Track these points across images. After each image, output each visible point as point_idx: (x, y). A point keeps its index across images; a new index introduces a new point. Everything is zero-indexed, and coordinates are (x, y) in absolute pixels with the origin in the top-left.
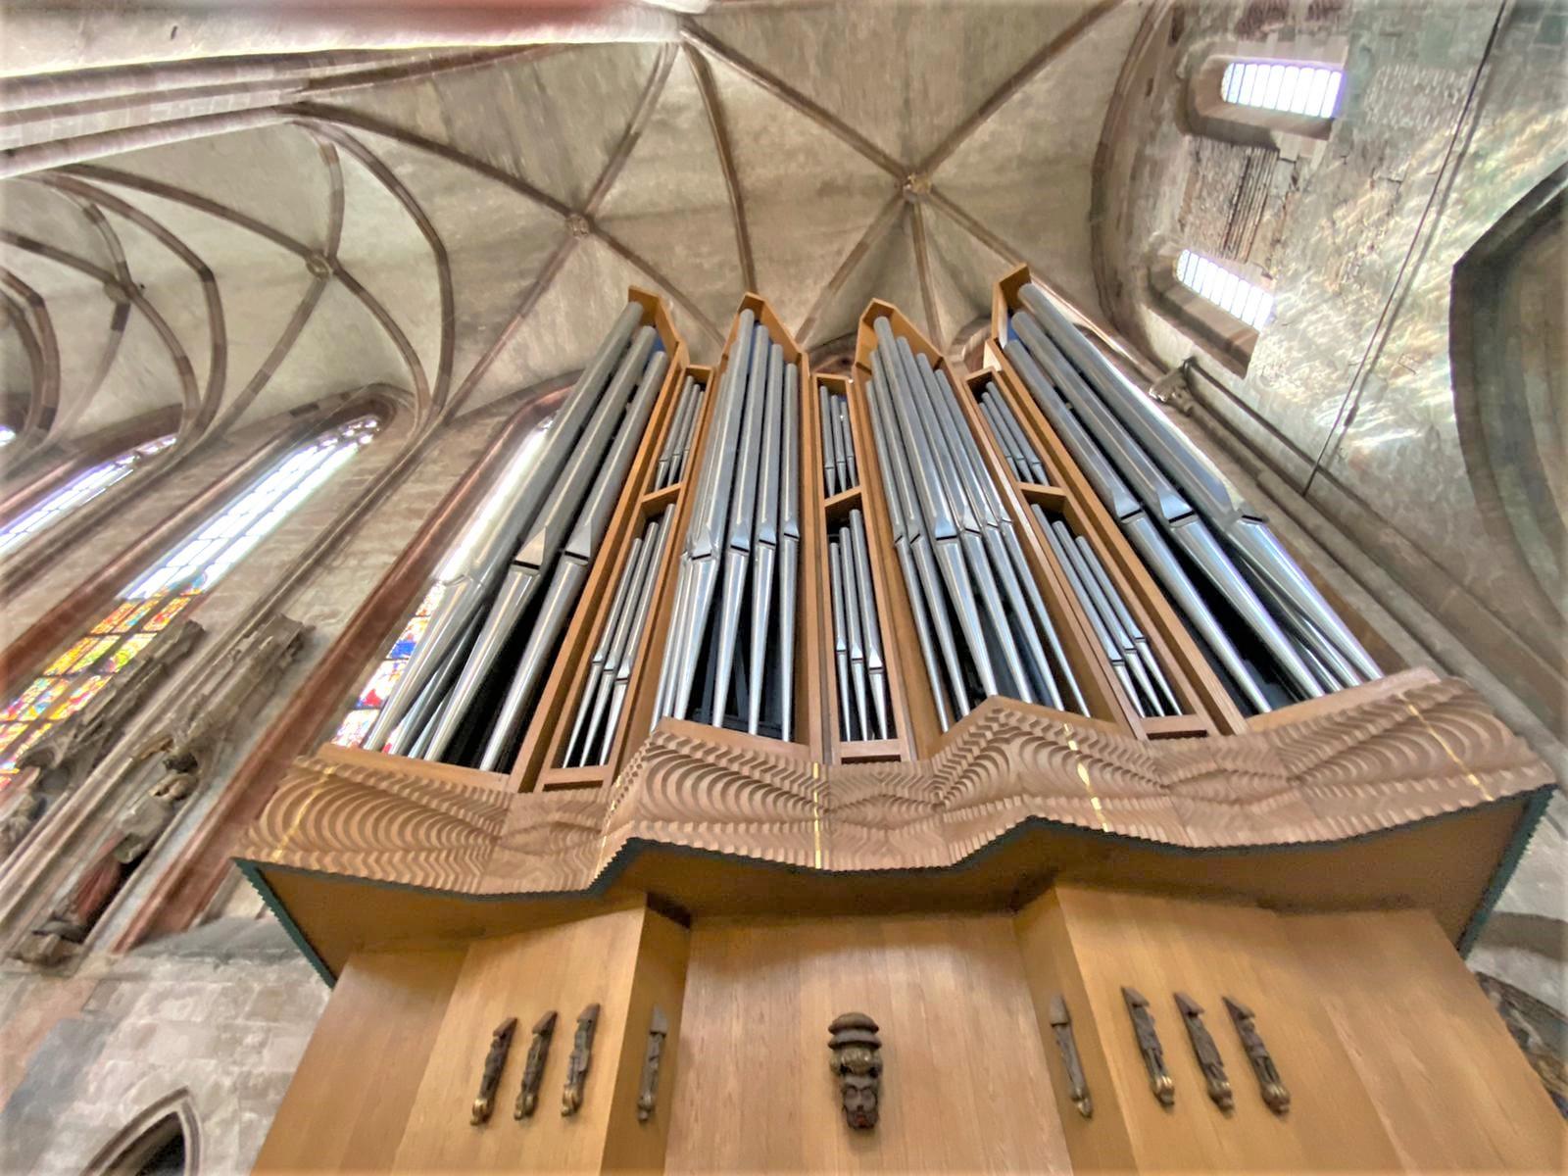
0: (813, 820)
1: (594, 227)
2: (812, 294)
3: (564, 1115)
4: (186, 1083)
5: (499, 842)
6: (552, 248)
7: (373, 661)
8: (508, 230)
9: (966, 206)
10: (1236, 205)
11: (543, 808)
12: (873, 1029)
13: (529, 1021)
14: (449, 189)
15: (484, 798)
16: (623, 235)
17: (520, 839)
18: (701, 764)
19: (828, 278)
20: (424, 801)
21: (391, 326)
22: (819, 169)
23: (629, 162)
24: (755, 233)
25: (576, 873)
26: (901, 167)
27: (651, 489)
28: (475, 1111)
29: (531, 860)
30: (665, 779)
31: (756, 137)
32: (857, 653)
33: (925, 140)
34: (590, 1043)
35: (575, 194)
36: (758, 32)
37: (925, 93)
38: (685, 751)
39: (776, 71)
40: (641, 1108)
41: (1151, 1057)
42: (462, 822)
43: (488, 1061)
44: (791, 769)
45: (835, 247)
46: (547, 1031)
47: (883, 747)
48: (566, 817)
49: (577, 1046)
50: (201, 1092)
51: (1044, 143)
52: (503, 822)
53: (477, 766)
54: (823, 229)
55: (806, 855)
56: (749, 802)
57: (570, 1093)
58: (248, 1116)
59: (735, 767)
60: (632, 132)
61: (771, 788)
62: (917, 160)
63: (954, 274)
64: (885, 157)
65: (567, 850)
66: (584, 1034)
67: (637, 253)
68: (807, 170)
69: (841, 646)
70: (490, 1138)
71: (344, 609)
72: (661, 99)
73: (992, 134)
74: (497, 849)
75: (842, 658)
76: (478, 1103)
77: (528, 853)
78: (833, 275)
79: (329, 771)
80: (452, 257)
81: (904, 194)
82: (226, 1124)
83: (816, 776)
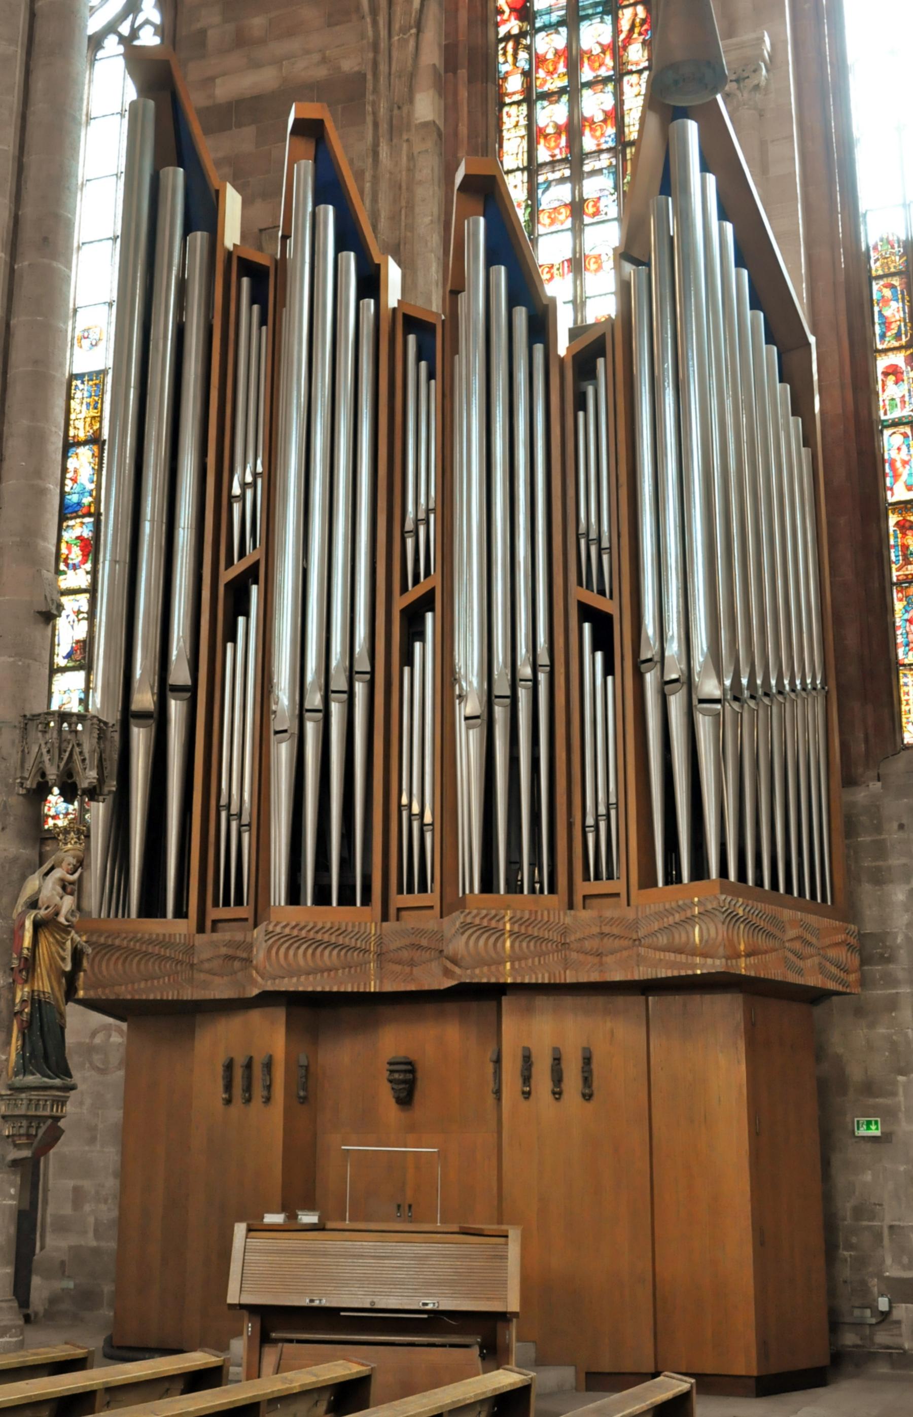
0: (370, 962)
3: (264, 1102)
5: (195, 967)
12: (410, 1063)
15: (178, 940)
17: (207, 966)
18: (297, 939)
20: (144, 949)
27: (230, 563)
28: (223, 1099)
29: (217, 980)
30: (277, 953)
32: (416, 809)
38: (287, 931)
41: (527, 1079)
42: (169, 958)
43: (224, 1078)
44: (356, 930)
46: (249, 1066)
48: (230, 952)
49: (264, 1075)
52: (193, 954)
55: (365, 984)
56: (329, 957)
59: (319, 937)
61: (343, 947)
65: (236, 973)
66: (265, 1069)
69: (405, 800)
74: (195, 971)
75: (405, 814)
76: (224, 1096)
83: (373, 932)
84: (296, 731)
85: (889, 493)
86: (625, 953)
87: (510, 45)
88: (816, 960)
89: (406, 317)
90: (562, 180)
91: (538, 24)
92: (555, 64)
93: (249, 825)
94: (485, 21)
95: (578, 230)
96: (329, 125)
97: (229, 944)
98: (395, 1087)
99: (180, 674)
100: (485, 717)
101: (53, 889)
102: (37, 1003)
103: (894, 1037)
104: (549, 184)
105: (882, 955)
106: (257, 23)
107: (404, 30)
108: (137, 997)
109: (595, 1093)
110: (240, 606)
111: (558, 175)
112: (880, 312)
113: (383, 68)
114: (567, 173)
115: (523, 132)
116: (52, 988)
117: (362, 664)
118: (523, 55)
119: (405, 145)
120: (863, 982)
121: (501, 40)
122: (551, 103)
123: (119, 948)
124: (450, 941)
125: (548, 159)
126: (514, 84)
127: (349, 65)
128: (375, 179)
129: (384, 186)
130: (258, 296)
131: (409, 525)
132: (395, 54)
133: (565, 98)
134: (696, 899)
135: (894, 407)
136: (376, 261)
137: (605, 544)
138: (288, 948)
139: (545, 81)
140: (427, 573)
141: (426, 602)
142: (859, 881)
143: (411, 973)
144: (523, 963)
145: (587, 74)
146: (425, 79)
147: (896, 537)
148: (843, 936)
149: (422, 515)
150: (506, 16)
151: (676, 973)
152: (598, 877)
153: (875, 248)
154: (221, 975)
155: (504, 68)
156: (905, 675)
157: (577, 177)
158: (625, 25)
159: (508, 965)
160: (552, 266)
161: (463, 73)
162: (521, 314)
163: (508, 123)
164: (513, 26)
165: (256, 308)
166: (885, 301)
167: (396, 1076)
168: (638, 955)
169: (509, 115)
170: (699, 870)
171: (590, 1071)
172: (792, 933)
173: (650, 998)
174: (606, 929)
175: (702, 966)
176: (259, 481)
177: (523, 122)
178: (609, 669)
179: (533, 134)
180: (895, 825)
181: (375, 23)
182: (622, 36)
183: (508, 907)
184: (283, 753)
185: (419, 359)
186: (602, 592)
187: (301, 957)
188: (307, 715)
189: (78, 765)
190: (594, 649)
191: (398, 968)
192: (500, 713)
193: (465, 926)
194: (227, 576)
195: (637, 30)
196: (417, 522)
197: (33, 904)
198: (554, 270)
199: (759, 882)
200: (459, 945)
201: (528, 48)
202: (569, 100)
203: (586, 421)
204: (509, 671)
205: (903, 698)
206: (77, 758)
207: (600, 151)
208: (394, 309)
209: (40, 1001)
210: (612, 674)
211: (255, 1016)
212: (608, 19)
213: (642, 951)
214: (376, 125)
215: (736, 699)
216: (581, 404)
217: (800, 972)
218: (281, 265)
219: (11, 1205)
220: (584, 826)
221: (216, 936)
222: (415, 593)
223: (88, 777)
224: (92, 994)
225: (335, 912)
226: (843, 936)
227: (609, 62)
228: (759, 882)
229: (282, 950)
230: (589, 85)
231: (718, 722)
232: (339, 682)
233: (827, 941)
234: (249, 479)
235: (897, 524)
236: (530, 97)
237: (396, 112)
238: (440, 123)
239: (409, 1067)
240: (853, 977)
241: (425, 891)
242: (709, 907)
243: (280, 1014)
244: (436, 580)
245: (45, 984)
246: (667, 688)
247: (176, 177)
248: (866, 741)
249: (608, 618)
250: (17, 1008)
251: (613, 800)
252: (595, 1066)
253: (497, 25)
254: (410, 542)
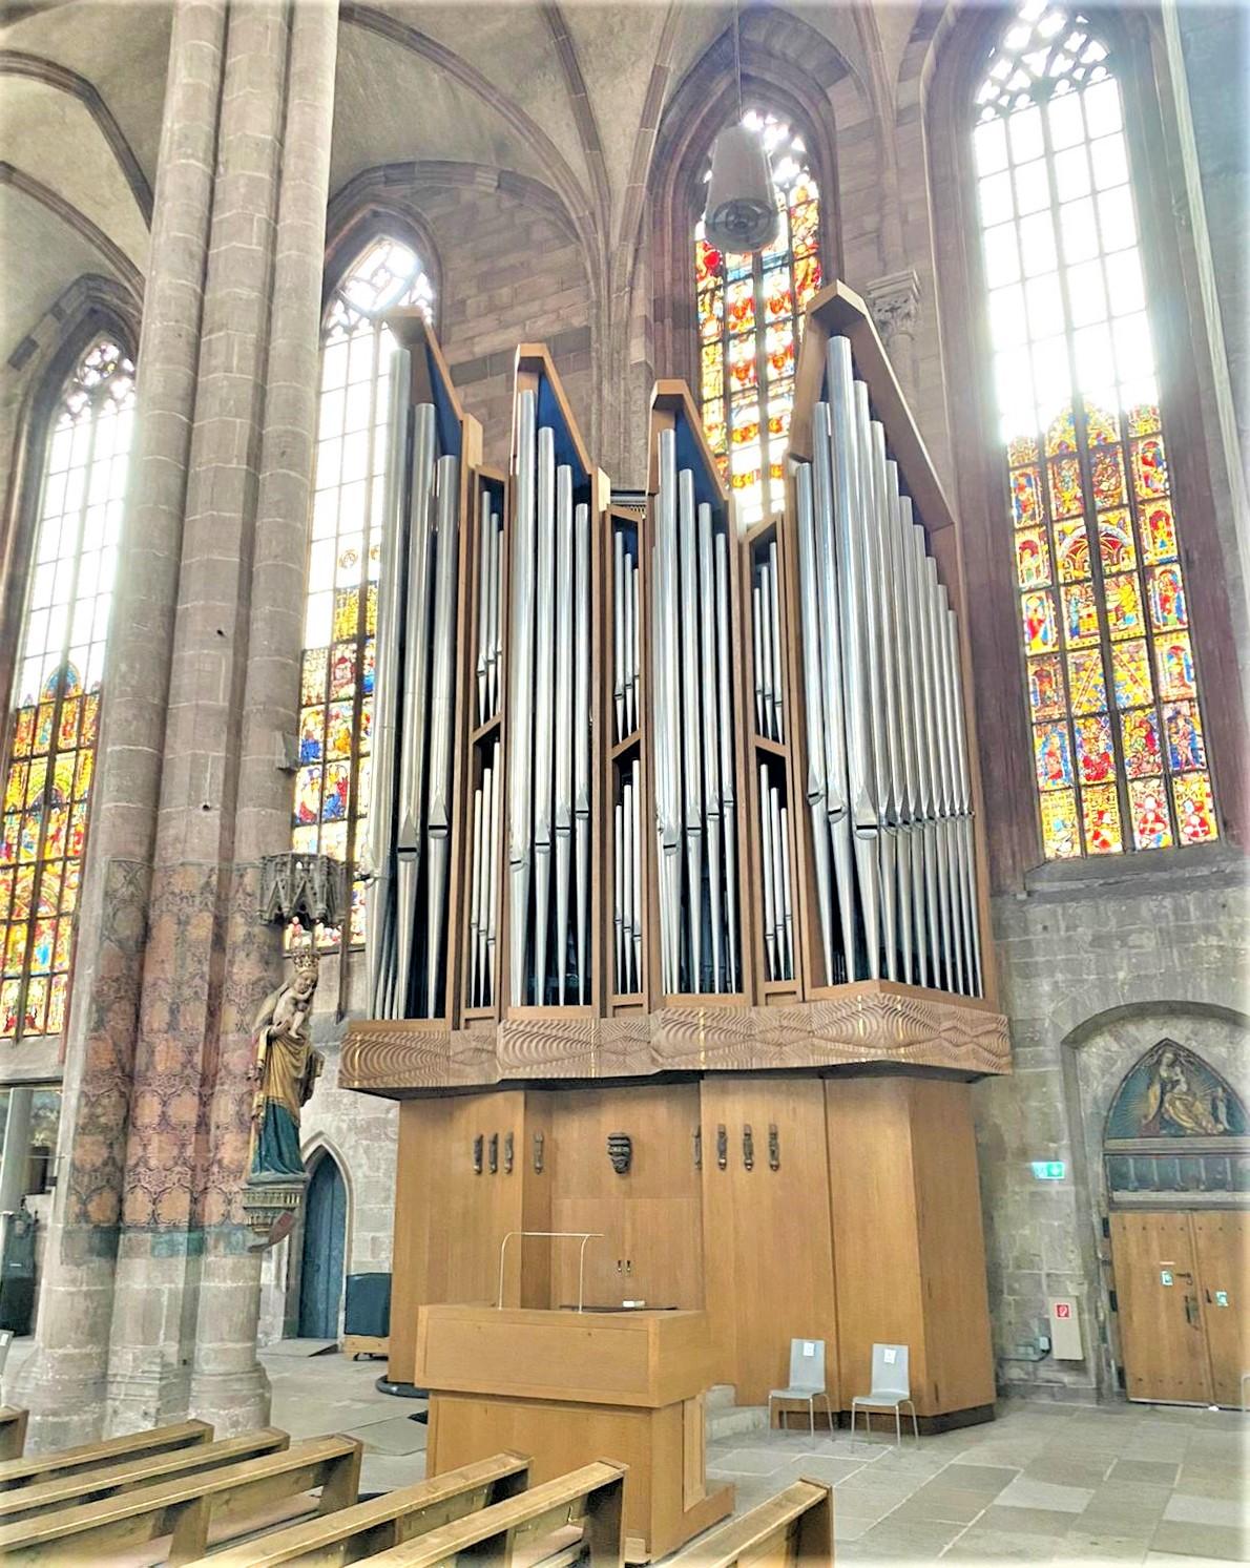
4: (322, 1129)
12: (628, 1139)
17: (460, 1057)
21: (76, 220)
27: (477, 725)
38: (521, 1028)
41: (723, 1153)
46: (495, 1142)
50: (331, 1132)
53: (427, 1017)
56: (556, 1049)
58: (365, 1142)
65: (482, 1063)
79: (359, 1038)
82: (355, 1147)
84: (528, 862)
85: (1027, 648)
87: (708, 295)
88: (971, 1046)
89: (614, 518)
90: (751, 404)
91: (730, 279)
92: (744, 309)
93: (494, 939)
94: (686, 281)
95: (765, 442)
96: (548, 362)
97: (477, 1039)
98: (616, 1159)
99: (437, 816)
100: (680, 846)
101: (285, 1008)
102: (271, 1107)
103: (1046, 1110)
104: (740, 408)
105: (1032, 1039)
106: (505, 293)
107: (619, 289)
108: (403, 1085)
109: (782, 1163)
110: (488, 762)
111: (747, 401)
112: (1017, 497)
113: (604, 320)
114: (755, 398)
115: (720, 367)
116: (284, 1093)
117: (582, 805)
118: (718, 305)
119: (622, 382)
120: (1014, 1064)
121: (700, 294)
122: (741, 342)
123: (388, 1044)
124: (655, 1034)
125: (739, 388)
126: (710, 330)
127: (578, 322)
128: (600, 411)
129: (606, 416)
130: (497, 507)
131: (619, 690)
132: (613, 309)
133: (753, 337)
134: (859, 998)
135: (1030, 576)
136: (589, 472)
137: (778, 698)
138: (523, 1042)
139: (734, 327)
140: (634, 728)
141: (633, 752)
142: (1010, 975)
144: (715, 1052)
145: (769, 317)
146: (637, 328)
147: (1034, 684)
148: (995, 1025)
149: (629, 681)
150: (703, 274)
151: (845, 1062)
152: (778, 978)
153: (1012, 446)
154: (471, 1065)
155: (702, 316)
156: (1046, 800)
157: (763, 400)
158: (800, 275)
159: (703, 1054)
160: (743, 477)
161: (668, 321)
162: (705, 509)
163: (706, 360)
164: (709, 282)
165: (495, 516)
166: (1021, 488)
167: (615, 1149)
168: (813, 1045)
169: (707, 354)
170: (863, 973)
171: (776, 1145)
172: (947, 1024)
173: (827, 1082)
174: (785, 1023)
175: (866, 1056)
176: (500, 658)
177: (719, 359)
178: (782, 803)
179: (727, 370)
180: (1040, 927)
181: (597, 285)
182: (798, 284)
183: (702, 1005)
184: (518, 879)
185: (625, 552)
186: (775, 739)
187: (534, 1049)
188: (537, 848)
189: (310, 899)
190: (770, 787)
191: (614, 1057)
192: (693, 842)
193: (666, 1021)
194: (474, 737)
195: (809, 278)
196: (625, 686)
197: (270, 1022)
198: (746, 479)
199: (916, 981)
200: (660, 1037)
201: (722, 298)
202: (756, 339)
203: (761, 596)
204: (699, 808)
205: (1045, 819)
206: (308, 892)
207: (782, 379)
208: (604, 512)
209: (274, 1106)
210: (786, 806)
211: (499, 1097)
212: (786, 270)
213: (816, 1041)
214: (600, 368)
215: (891, 824)
216: (756, 582)
217: (956, 1059)
218: (513, 480)
219: (230, 1293)
220: (765, 935)
221: (467, 1032)
222: (624, 745)
223: (317, 909)
224: (365, 1085)
225: (562, 1011)
226: (995, 1025)
227: (788, 305)
228: (916, 981)
229: (518, 1044)
230: (772, 325)
231: (877, 844)
232: (563, 820)
233: (980, 1030)
234: (491, 657)
235: (1036, 673)
236: (725, 339)
237: (616, 355)
238: (651, 363)
239: (625, 1142)
240: (1004, 1060)
241: (636, 991)
242: (871, 1004)
243: (519, 1096)
244: (641, 734)
245: (277, 1090)
246: (831, 817)
247: (427, 411)
248: (1013, 856)
249: (782, 760)
250: (254, 1113)
251: (788, 912)
252: (780, 1140)
253: (696, 282)
254: (620, 704)
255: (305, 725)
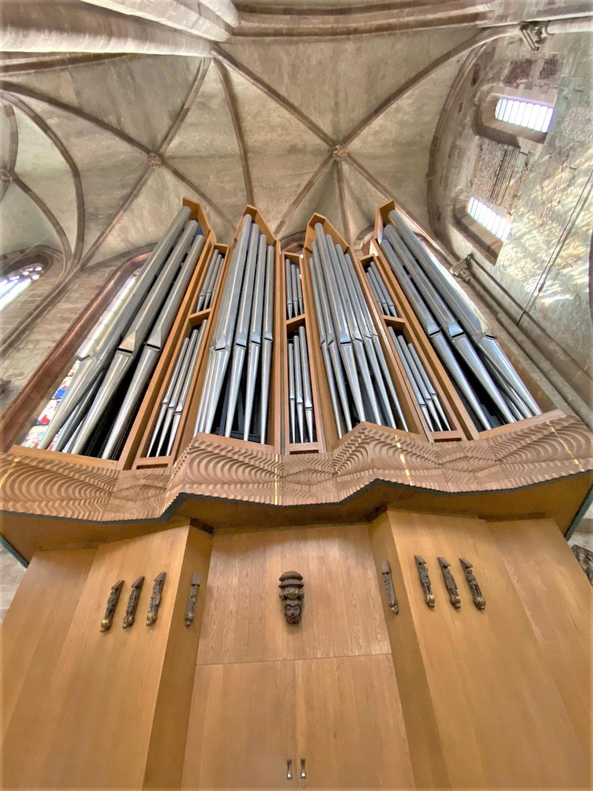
0: (275, 482)
1: (164, 162)
2: (284, 207)
3: (148, 625)
5: (113, 495)
6: (140, 172)
7: (45, 400)
8: (114, 160)
9: (366, 164)
10: (498, 175)
11: (136, 478)
12: (300, 578)
13: (130, 581)
14: (80, 134)
15: (104, 473)
16: (180, 167)
17: (124, 493)
18: (218, 456)
19: (292, 201)
22: (288, 138)
23: (183, 125)
24: (255, 173)
25: (154, 509)
26: (333, 141)
27: (194, 311)
28: (102, 626)
31: (255, 117)
32: (300, 400)
33: (345, 126)
34: (161, 590)
35: (153, 140)
36: (256, 55)
37: (346, 100)
38: (210, 449)
39: (266, 79)
40: (187, 620)
43: (109, 602)
44: (264, 457)
45: (296, 183)
46: (139, 586)
47: (311, 446)
48: (148, 482)
49: (154, 593)
51: (407, 134)
52: (114, 485)
53: (100, 457)
54: (290, 172)
55: (270, 499)
56: (242, 473)
57: (150, 615)
59: (236, 457)
60: (185, 107)
61: (254, 467)
62: (341, 138)
63: (358, 202)
64: (325, 134)
65: (149, 498)
66: (158, 587)
67: (188, 178)
68: (282, 138)
69: (292, 396)
70: (111, 637)
71: (26, 372)
72: (202, 89)
73: (380, 126)
74: (112, 498)
75: (293, 403)
76: (104, 621)
77: (128, 500)
78: (295, 198)
79: (17, 460)
80: (82, 174)
81: (334, 156)
83: (277, 460)
86: (493, 470)
143: (309, 491)
191: (298, 487)
255: (65, 383)
